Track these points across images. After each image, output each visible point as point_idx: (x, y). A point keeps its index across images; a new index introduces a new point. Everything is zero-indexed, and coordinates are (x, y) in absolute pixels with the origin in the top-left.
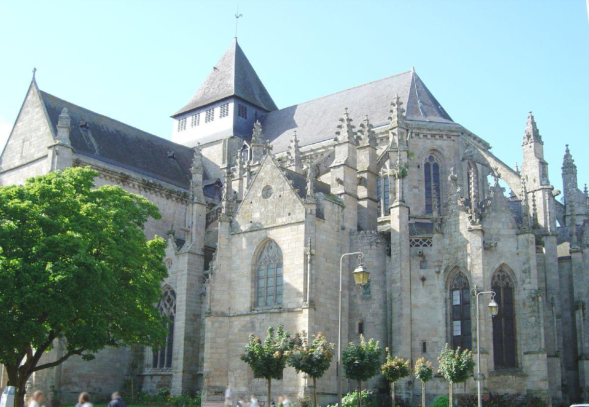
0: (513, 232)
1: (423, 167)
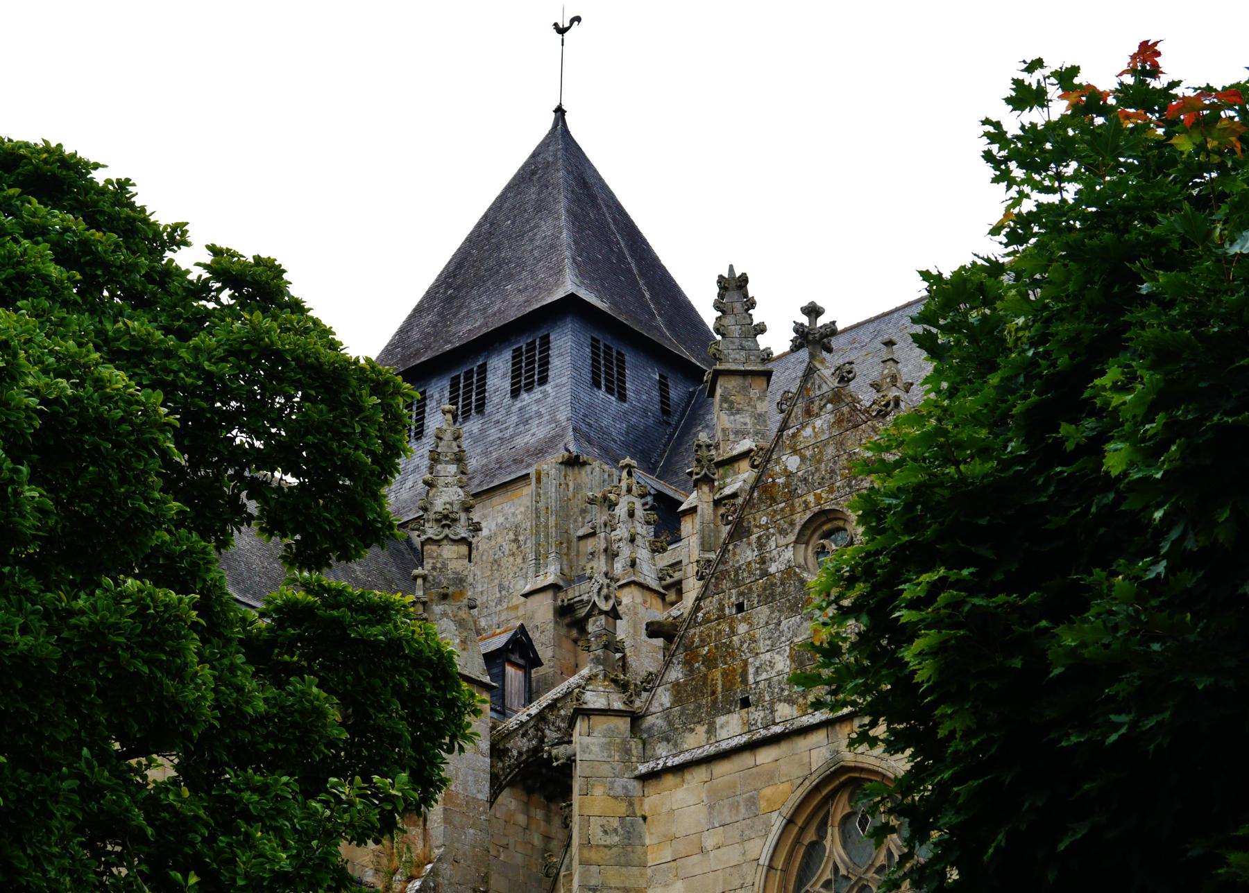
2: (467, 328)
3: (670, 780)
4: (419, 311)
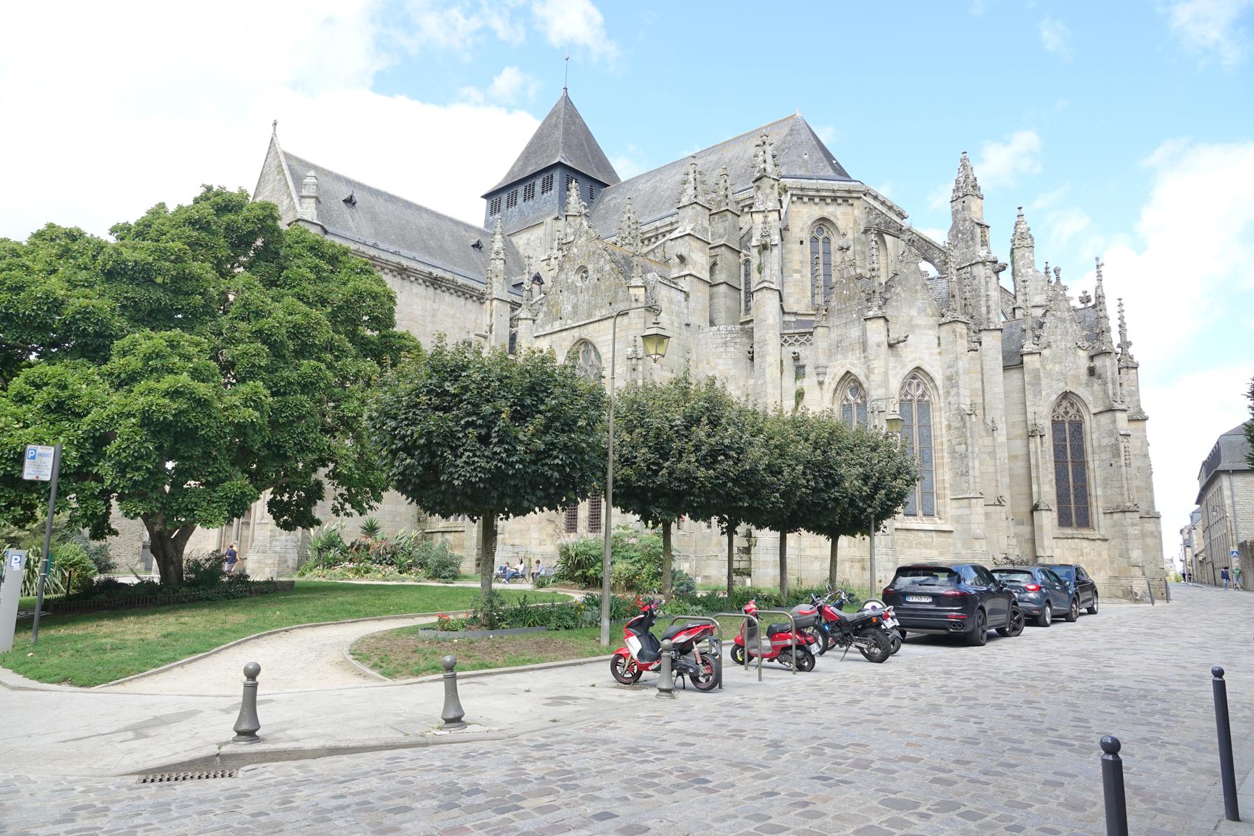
0: (932, 321)
1: (807, 243)
2: (530, 170)
3: (542, 338)
4: (518, 160)
